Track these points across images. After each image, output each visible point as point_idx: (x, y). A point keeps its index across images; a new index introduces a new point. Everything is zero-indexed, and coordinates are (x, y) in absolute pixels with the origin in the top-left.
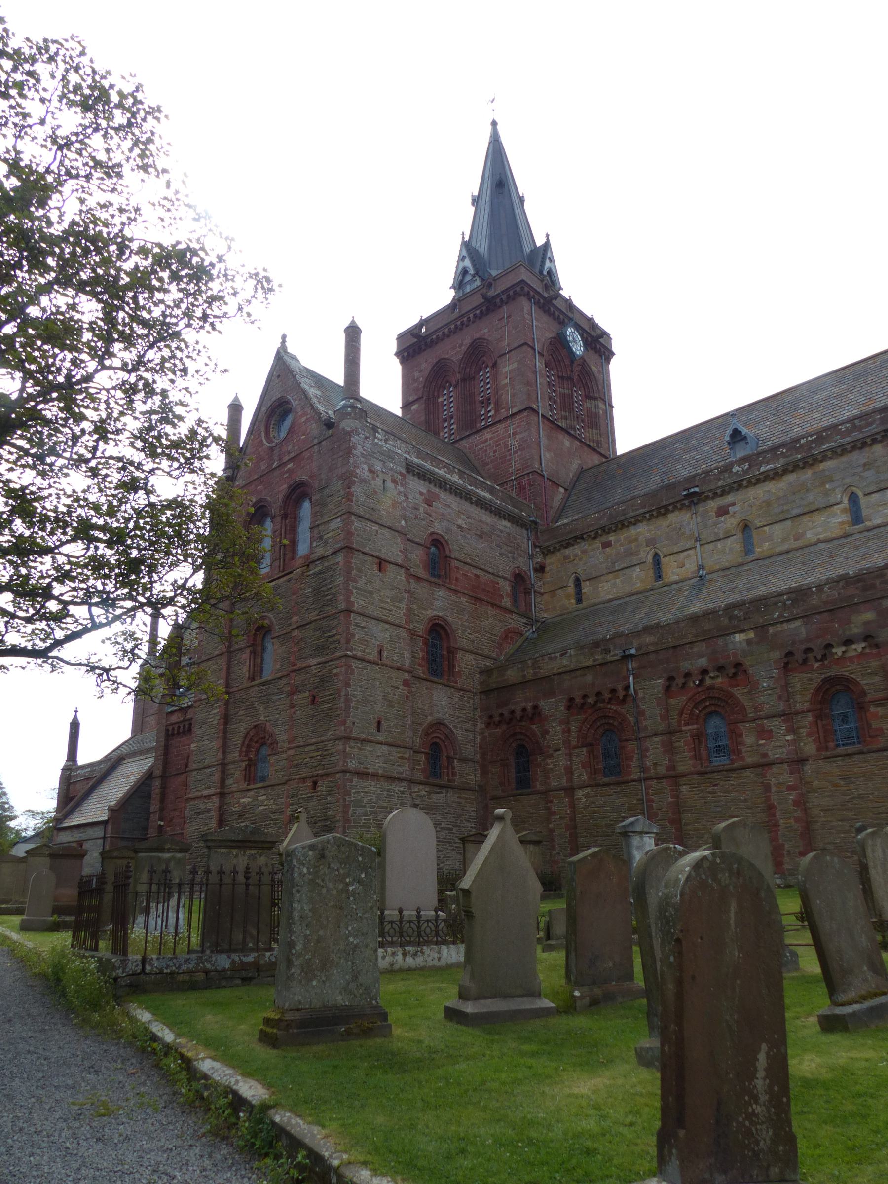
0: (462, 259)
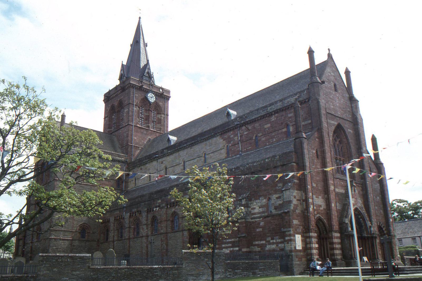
0: (121, 71)
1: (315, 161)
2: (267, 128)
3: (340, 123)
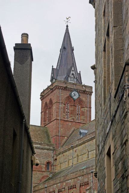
0: (52, 74)
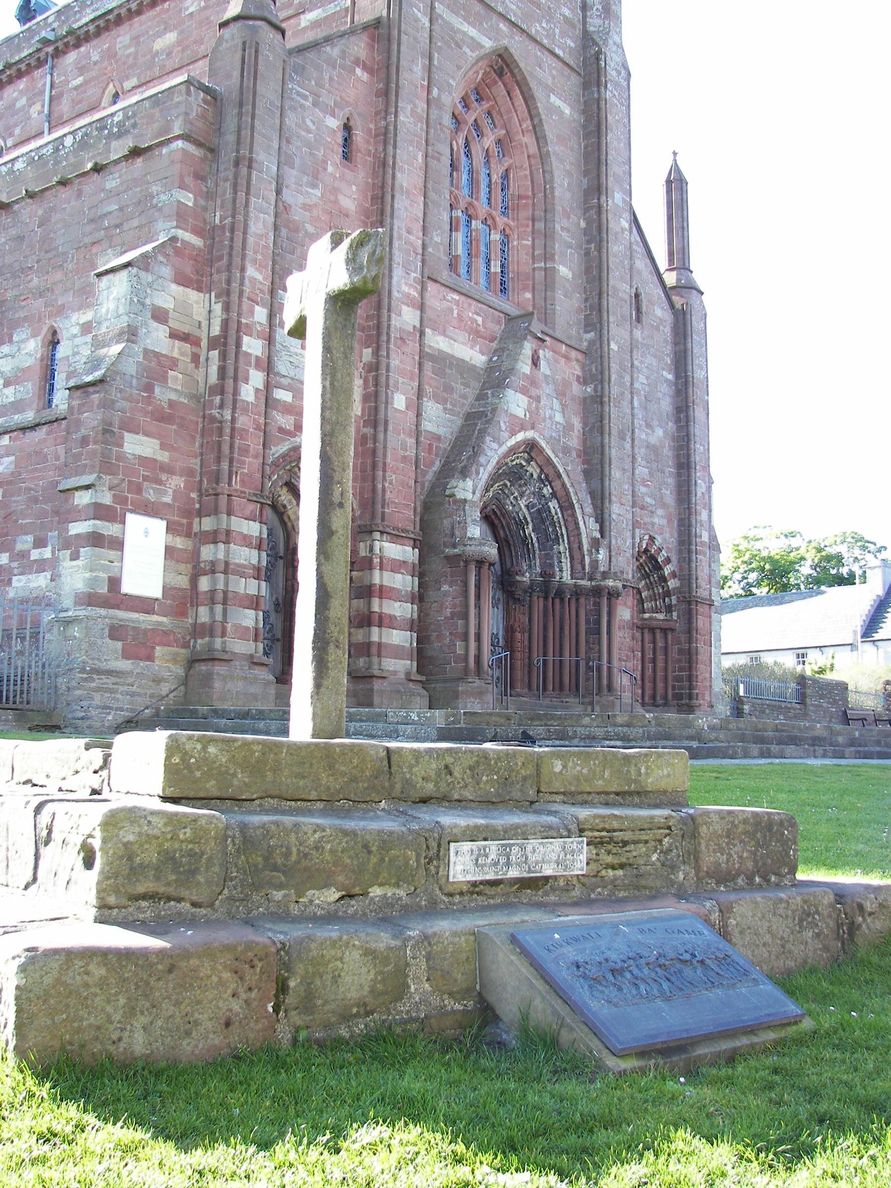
1: (330, 169)
2: (163, 51)
3: (512, 51)
